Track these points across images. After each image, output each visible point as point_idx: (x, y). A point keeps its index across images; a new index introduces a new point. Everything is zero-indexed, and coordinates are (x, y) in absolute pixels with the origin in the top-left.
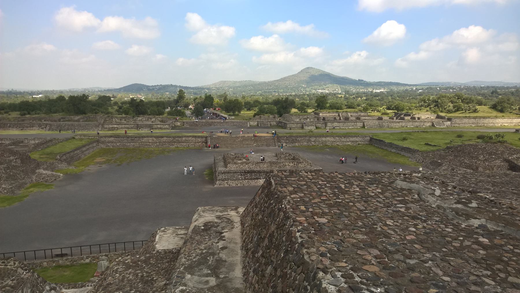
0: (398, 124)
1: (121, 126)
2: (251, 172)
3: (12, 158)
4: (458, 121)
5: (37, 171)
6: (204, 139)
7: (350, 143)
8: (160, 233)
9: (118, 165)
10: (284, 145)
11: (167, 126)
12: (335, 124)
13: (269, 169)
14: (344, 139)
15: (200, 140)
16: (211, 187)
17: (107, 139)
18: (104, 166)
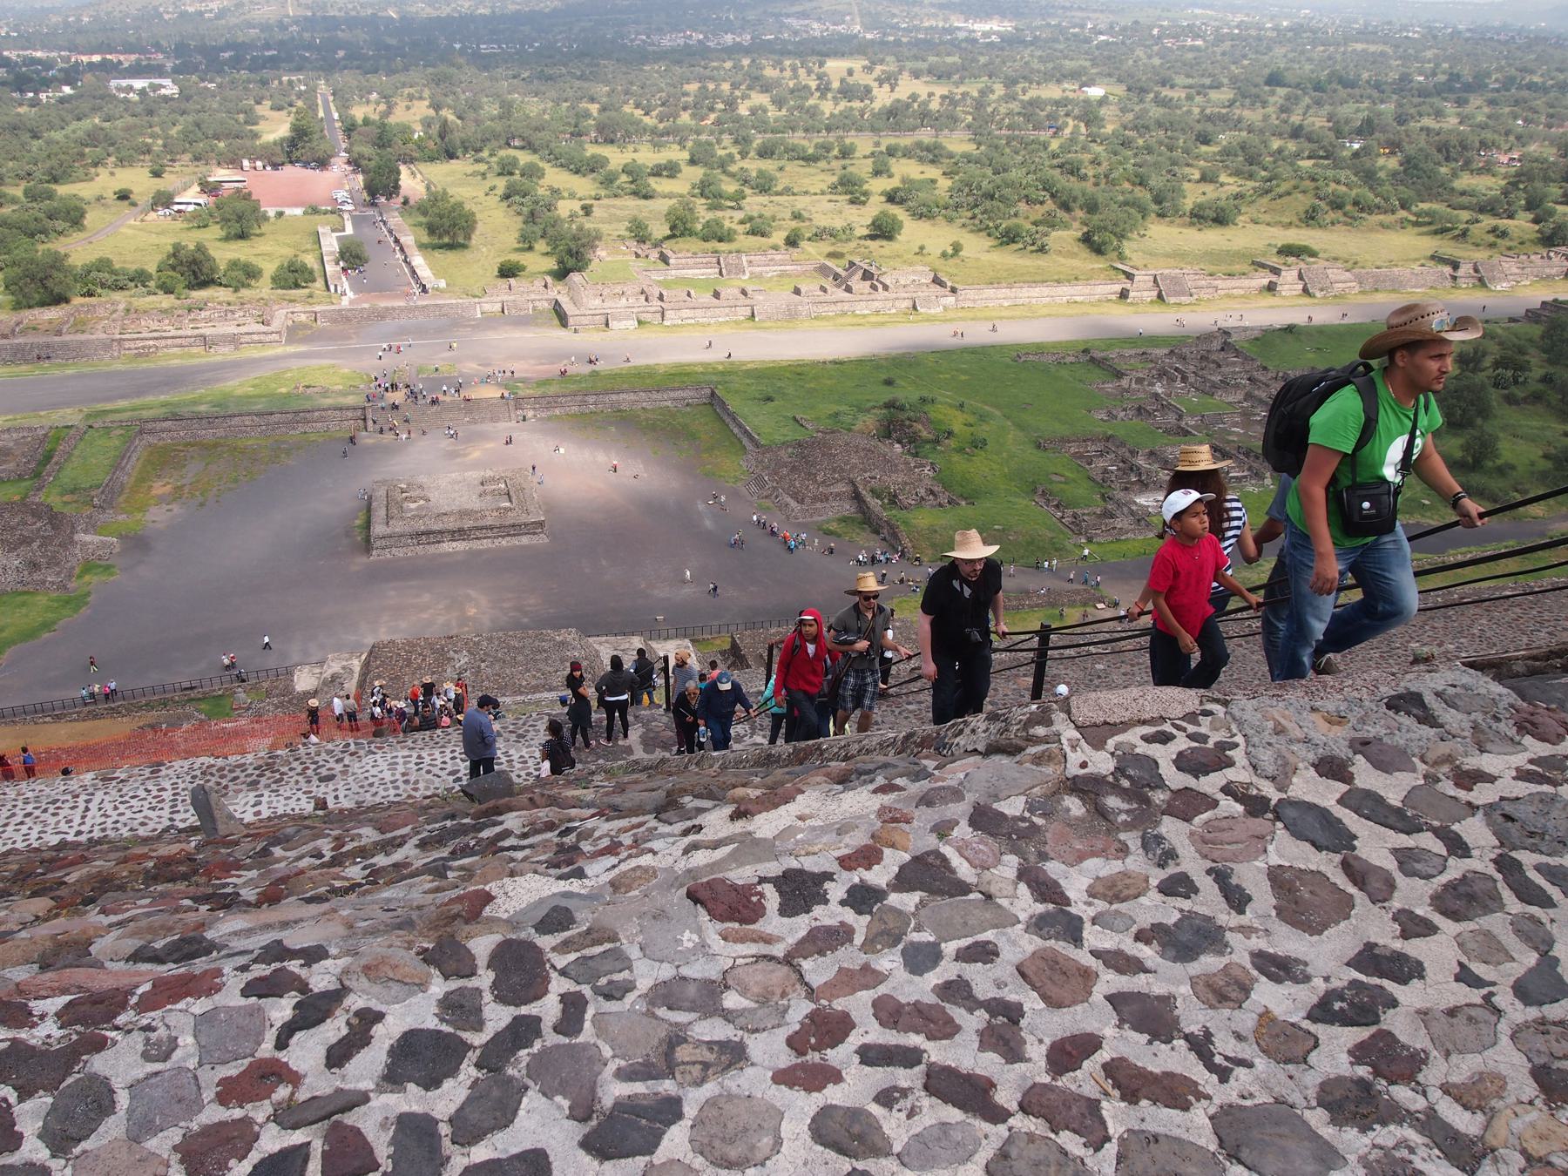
0: (833, 307)
1: (163, 343)
2: (428, 533)
3: (39, 524)
4: (971, 294)
5: (76, 537)
6: (359, 413)
7: (669, 403)
8: (297, 673)
9: (202, 505)
10: (530, 414)
11: (276, 337)
12: (686, 313)
13: (458, 525)
14: (655, 396)
15: (350, 414)
16: (363, 559)
17: (159, 425)
18: (176, 508)
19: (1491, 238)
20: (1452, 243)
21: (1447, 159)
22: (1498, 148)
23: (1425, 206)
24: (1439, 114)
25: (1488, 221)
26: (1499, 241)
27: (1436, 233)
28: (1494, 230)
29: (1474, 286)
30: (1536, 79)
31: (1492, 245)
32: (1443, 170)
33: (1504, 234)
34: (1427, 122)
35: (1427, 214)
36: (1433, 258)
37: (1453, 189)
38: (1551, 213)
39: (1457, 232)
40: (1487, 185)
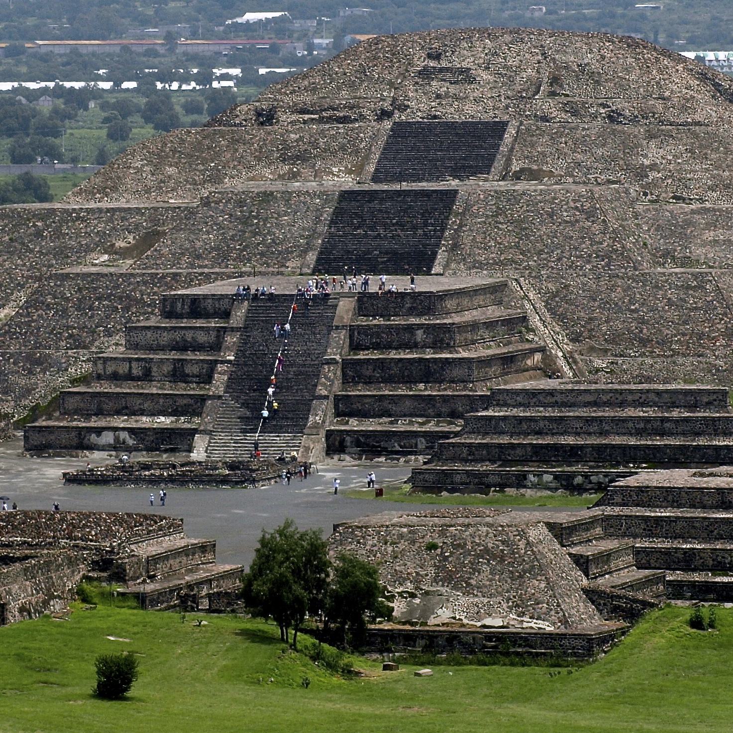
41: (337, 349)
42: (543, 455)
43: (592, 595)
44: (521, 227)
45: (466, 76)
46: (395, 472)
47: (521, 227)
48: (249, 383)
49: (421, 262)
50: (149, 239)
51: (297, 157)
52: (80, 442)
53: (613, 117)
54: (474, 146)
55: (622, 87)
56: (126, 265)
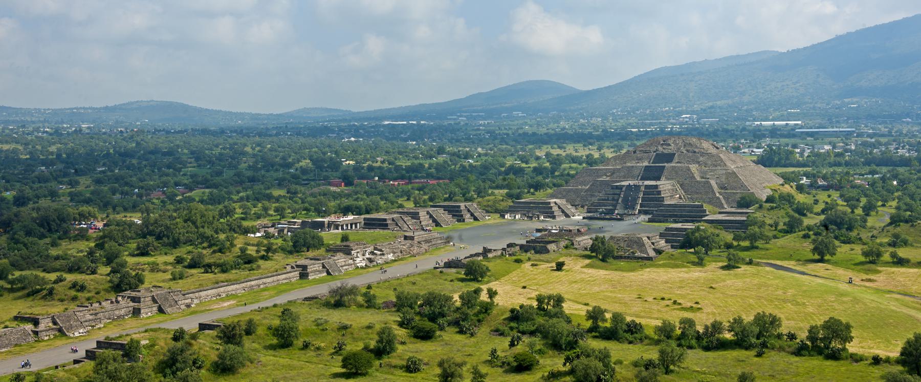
19: (73, 293)
20: (42, 302)
21: (50, 230)
22: (95, 218)
23: (17, 274)
24: (53, 194)
25: (70, 277)
26: (79, 294)
27: (28, 295)
28: (74, 286)
29: (55, 337)
30: (134, 161)
31: (74, 299)
32: (42, 242)
33: (82, 288)
34: (44, 203)
35: (20, 280)
36: (16, 318)
37: (48, 256)
38: (123, 265)
39: (45, 292)
40: (77, 249)
41: (641, 195)
42: (671, 216)
43: (654, 250)
44: (677, 173)
45: (669, 145)
46: (647, 217)
47: (677, 173)
48: (625, 201)
49: (658, 179)
50: (613, 173)
51: (640, 159)
52: (596, 211)
53: (695, 152)
54: (669, 158)
55: (696, 147)
56: (608, 179)
